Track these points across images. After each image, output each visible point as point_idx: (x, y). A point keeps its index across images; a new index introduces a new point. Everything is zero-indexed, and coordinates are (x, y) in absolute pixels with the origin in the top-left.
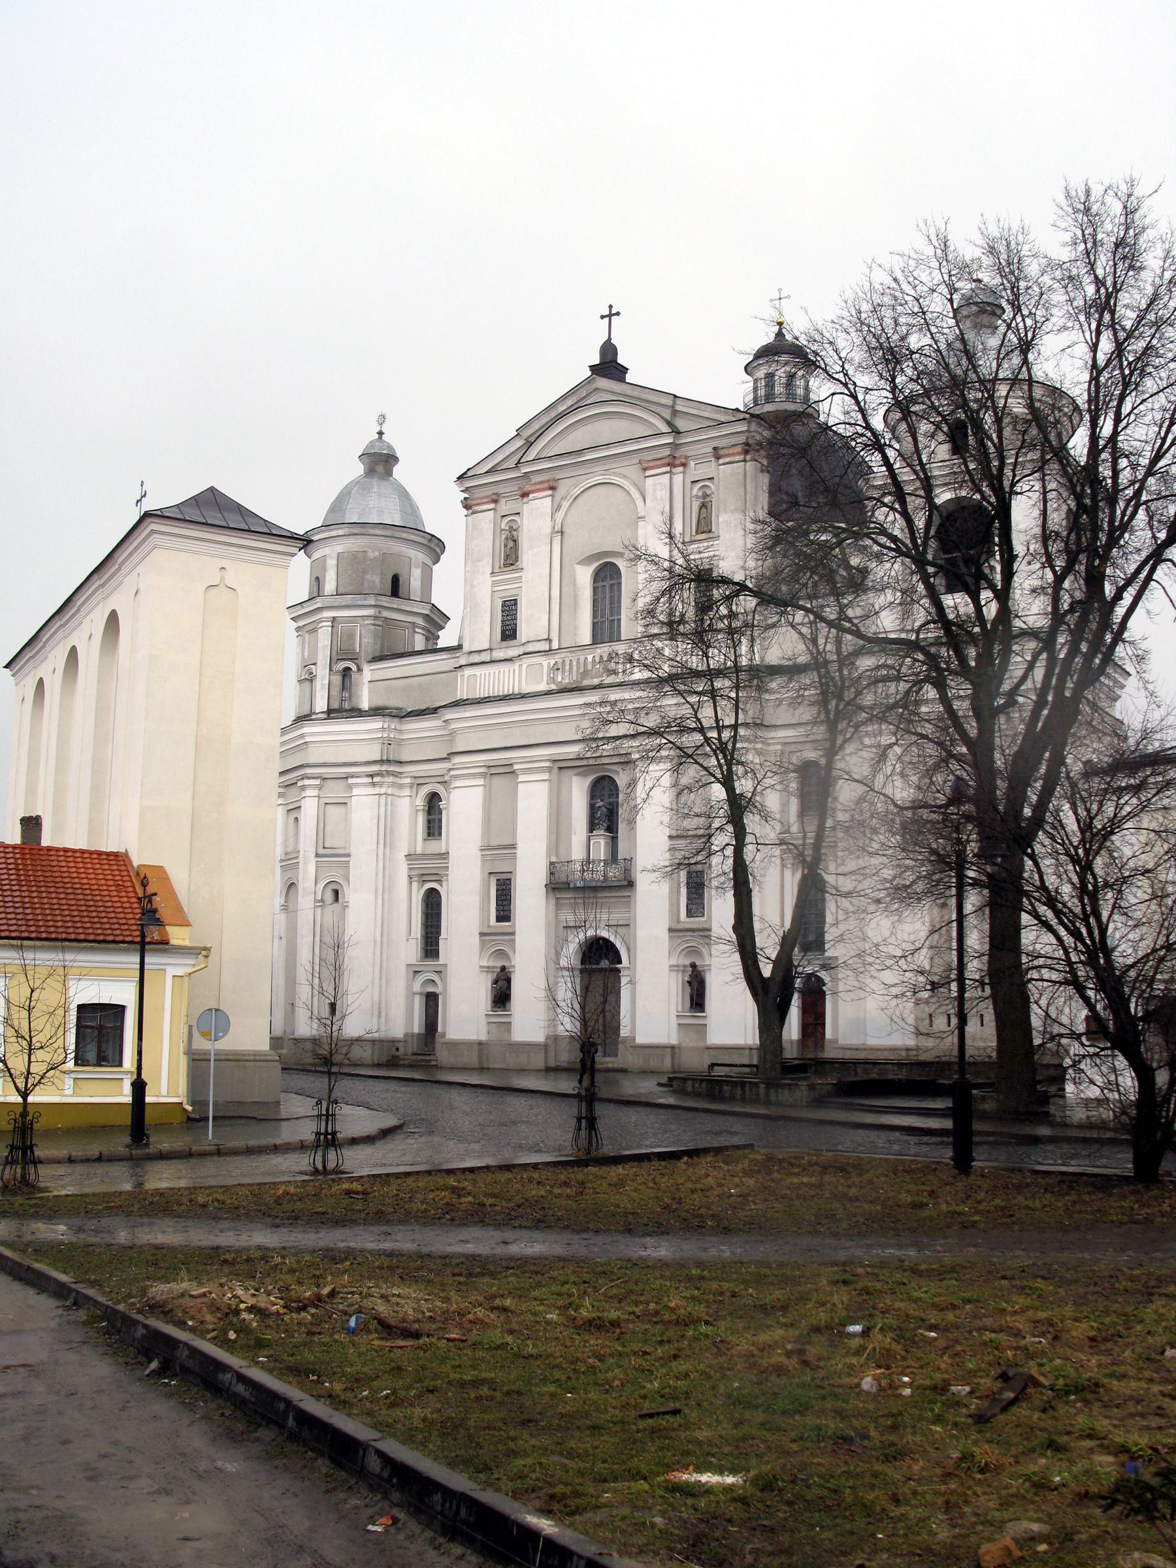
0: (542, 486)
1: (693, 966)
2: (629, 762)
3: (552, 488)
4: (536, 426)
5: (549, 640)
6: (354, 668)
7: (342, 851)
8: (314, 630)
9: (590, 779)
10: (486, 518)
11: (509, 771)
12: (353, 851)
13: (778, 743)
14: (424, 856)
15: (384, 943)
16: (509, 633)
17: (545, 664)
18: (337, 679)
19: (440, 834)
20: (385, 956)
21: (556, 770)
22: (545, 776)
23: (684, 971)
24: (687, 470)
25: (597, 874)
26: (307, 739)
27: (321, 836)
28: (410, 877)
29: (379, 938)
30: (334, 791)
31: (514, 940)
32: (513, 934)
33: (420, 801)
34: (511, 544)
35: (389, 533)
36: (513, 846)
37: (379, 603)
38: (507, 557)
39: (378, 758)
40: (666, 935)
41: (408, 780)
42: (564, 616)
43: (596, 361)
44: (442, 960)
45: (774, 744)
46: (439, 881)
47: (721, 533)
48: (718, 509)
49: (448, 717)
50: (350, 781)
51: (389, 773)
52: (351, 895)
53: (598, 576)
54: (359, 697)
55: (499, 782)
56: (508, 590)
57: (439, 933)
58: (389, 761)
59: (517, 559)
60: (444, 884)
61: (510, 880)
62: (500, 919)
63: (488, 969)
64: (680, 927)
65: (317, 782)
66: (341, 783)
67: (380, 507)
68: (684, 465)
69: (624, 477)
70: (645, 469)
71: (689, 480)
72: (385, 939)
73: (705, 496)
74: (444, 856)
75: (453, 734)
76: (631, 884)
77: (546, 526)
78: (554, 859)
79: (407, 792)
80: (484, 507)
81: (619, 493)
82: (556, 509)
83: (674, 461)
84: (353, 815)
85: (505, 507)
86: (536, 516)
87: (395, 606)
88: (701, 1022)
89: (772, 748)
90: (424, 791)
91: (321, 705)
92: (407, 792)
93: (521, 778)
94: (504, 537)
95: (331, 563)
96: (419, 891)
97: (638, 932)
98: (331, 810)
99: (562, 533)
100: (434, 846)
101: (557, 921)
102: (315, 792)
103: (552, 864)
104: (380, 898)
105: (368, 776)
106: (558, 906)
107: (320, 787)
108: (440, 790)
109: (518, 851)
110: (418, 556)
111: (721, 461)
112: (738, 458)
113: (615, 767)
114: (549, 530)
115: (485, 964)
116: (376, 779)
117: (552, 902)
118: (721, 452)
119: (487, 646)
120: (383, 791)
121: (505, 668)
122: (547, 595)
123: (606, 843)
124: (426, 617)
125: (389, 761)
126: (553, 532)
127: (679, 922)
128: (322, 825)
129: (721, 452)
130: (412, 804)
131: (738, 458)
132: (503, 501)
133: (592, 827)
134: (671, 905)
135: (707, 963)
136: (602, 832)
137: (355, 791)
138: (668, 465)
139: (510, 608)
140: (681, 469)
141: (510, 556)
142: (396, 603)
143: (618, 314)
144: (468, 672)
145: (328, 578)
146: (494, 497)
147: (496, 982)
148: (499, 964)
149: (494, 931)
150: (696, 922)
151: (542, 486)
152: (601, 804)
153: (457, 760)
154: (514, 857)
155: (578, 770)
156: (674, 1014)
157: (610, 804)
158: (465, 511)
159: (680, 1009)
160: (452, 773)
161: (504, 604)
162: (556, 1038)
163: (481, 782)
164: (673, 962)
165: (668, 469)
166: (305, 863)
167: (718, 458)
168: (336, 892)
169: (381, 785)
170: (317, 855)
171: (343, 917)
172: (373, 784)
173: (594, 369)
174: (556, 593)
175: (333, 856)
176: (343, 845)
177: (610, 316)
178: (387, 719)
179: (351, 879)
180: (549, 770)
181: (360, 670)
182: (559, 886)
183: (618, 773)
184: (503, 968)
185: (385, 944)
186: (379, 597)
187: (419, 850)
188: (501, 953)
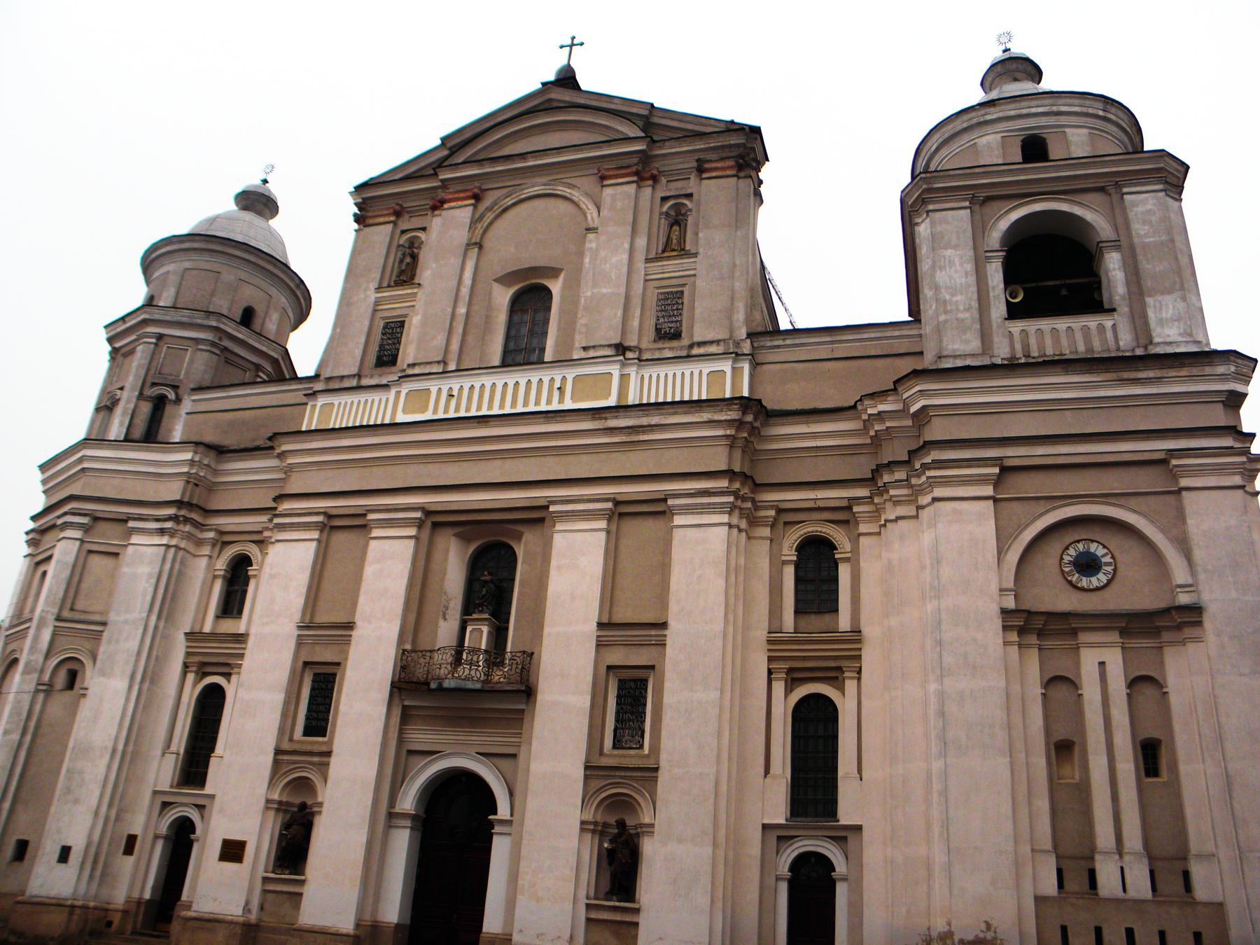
0: (462, 195)
1: (621, 824)
3: (477, 198)
4: (467, 135)
5: (444, 362)
6: (172, 396)
7: (97, 618)
8: (132, 352)
10: (381, 234)
11: (359, 524)
12: (112, 617)
13: (772, 507)
14: (213, 636)
15: (129, 754)
16: (387, 357)
17: (434, 390)
18: (146, 408)
19: (240, 612)
20: (124, 775)
21: (428, 524)
22: (412, 531)
23: (602, 834)
24: (658, 187)
25: (472, 674)
26: (86, 465)
27: (71, 594)
28: (186, 666)
29: (120, 747)
30: (107, 536)
31: (328, 764)
33: (221, 564)
34: (408, 260)
35: (252, 258)
36: (350, 626)
37: (222, 326)
38: (401, 272)
39: (178, 497)
40: (581, 773)
41: (211, 535)
42: (470, 339)
43: (552, 78)
44: (208, 790)
45: (766, 508)
46: (227, 676)
47: (701, 250)
48: (697, 225)
49: (285, 448)
50: (131, 524)
51: (187, 520)
52: (92, 680)
53: (517, 304)
54: (170, 431)
55: (340, 538)
56: (393, 309)
57: (212, 749)
58: (190, 506)
59: (413, 276)
60: (234, 678)
61: (335, 675)
62: (308, 732)
63: (281, 807)
65: (85, 520)
66: (118, 528)
67: (248, 228)
68: (655, 179)
69: (572, 186)
70: (603, 178)
71: (660, 193)
72: (130, 748)
73: (678, 213)
74: (241, 638)
75: (289, 470)
76: (528, 692)
77: (460, 235)
78: (408, 647)
79: (206, 550)
80: (381, 220)
81: (563, 206)
82: (474, 222)
83: (643, 170)
84: (126, 569)
85: (404, 225)
86: (447, 229)
87: (240, 336)
88: (628, 918)
89: (763, 513)
90: (230, 552)
91: (116, 429)
92: (206, 550)
94: (400, 254)
95: (173, 279)
96: (195, 685)
97: (534, 766)
98: (95, 561)
99: (480, 247)
100: (228, 626)
101: (401, 740)
102: (78, 534)
104: (136, 688)
105: (158, 520)
106: (407, 717)
107: (87, 529)
108: (253, 551)
109: (355, 633)
110: (283, 300)
111: (704, 176)
112: (729, 172)
113: (519, 528)
114: (465, 241)
115: (276, 797)
116: (168, 525)
117: (397, 712)
118: (707, 166)
119: (354, 370)
120: (174, 542)
121: (376, 396)
122: (450, 310)
123: (490, 633)
124: (275, 362)
125: (190, 506)
126: (469, 245)
127: (601, 753)
128: (76, 579)
129: (707, 166)
130: (210, 567)
131: (729, 172)
132: (406, 216)
133: (469, 608)
134: (591, 726)
135: (647, 820)
137: (135, 539)
138: (637, 173)
139: (393, 331)
140: (650, 182)
141: (405, 270)
142: (242, 333)
143: (582, 44)
144: (321, 401)
145: (165, 294)
146: (398, 208)
147: (287, 826)
148: (297, 801)
149: (296, 747)
150: (629, 758)
151: (462, 195)
152: (488, 578)
153: (286, 506)
154: (347, 640)
155: (459, 530)
156: (583, 902)
157: (501, 580)
158: (356, 226)
159: (592, 894)
160: (276, 521)
161: (386, 326)
163: (316, 535)
164: (589, 816)
165: (635, 178)
166: (39, 628)
167: (700, 170)
168: (73, 678)
169: (172, 533)
170: (59, 619)
171: (73, 711)
172: (162, 532)
173: (544, 84)
174: (462, 310)
175: (79, 625)
176: (96, 608)
178: (201, 449)
179: (100, 657)
180: (420, 524)
181: (178, 400)
182: (412, 688)
183: (518, 537)
184: (303, 806)
185: (128, 758)
186: (224, 320)
187: (207, 628)
188: (304, 785)
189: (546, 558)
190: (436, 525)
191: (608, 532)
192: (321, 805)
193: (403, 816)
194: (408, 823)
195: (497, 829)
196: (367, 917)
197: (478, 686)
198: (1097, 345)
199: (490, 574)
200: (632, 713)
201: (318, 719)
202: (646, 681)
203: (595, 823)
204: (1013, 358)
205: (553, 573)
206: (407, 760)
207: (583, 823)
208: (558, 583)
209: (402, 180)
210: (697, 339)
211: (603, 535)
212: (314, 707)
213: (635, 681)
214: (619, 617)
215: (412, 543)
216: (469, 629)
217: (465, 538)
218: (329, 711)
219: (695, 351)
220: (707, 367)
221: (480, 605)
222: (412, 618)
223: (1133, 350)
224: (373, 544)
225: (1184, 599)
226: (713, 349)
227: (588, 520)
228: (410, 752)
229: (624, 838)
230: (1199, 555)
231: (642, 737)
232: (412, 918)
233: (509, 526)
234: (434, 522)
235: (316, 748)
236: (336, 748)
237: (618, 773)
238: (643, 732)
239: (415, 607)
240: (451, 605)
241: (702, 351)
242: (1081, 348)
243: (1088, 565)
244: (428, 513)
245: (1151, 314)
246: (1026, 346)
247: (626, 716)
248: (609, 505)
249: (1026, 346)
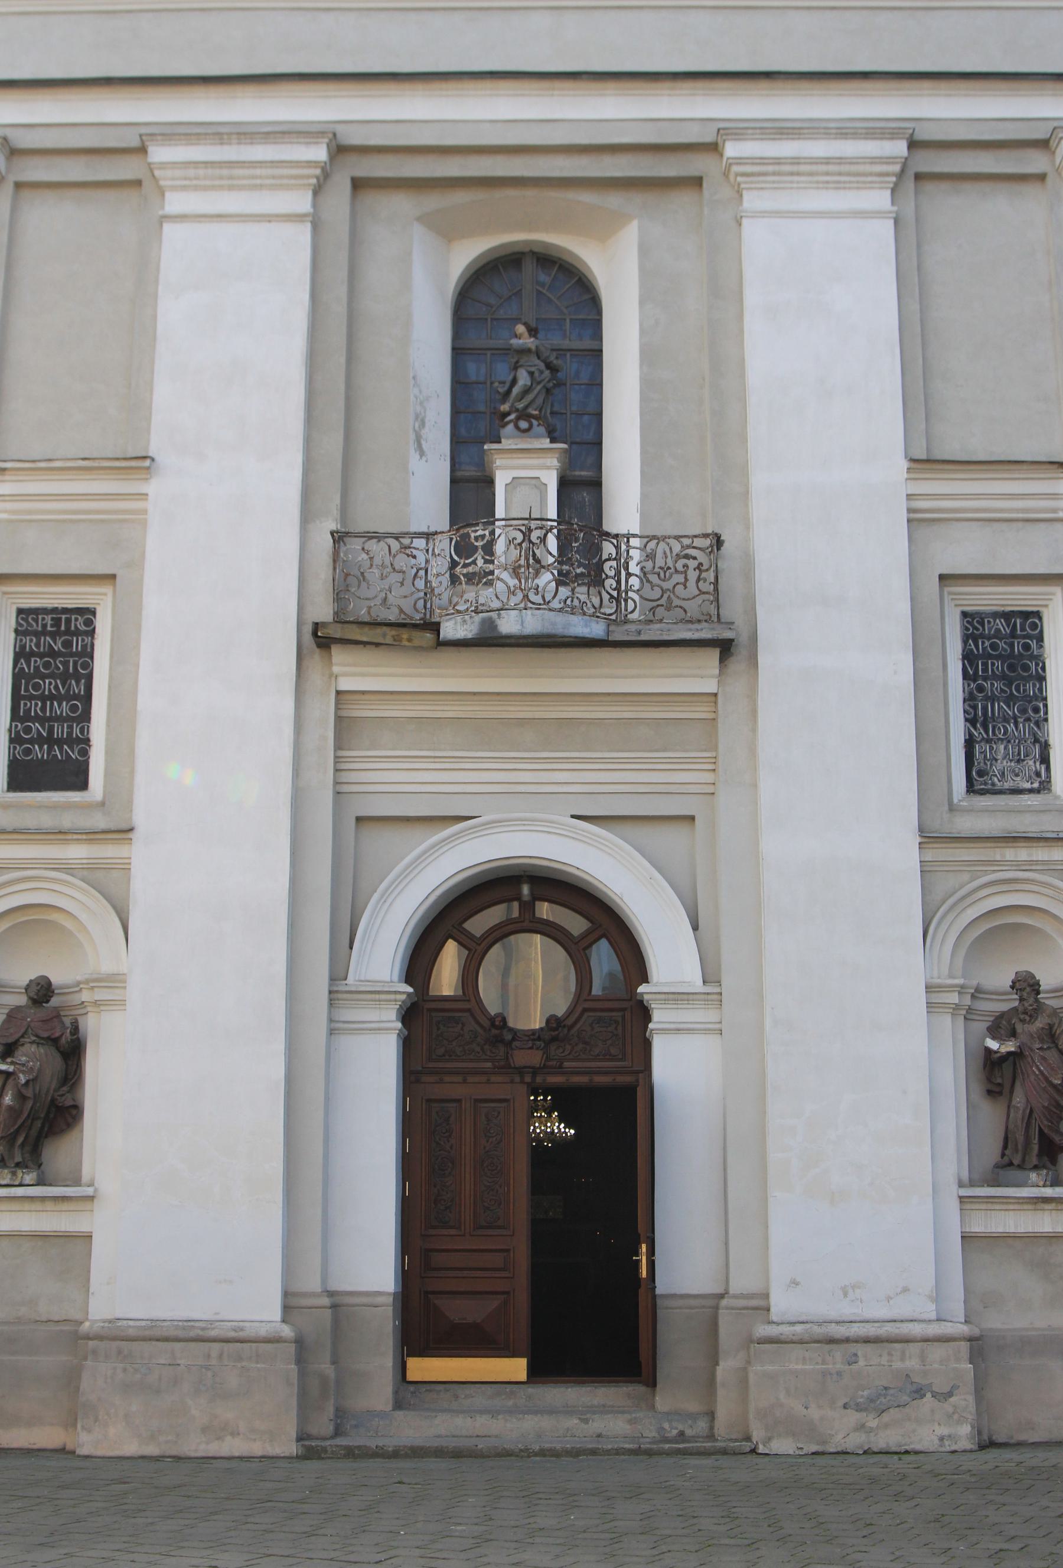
2: (697, 182)
9: (465, 255)
32: (125, 832)
61: (88, 614)
64: (965, 824)
93: (175, 203)
103: (339, 538)
106: (345, 729)
113: (614, 200)
117: (322, 710)
136: (546, 443)
155: (433, 201)
156: (951, 1192)
157: (560, 352)
162: (340, 1307)
183: (604, 228)
189: (724, 290)
190: (358, 185)
191: (896, 222)
192: (116, 980)
193: (374, 994)
194: (390, 1017)
195: (660, 1017)
196: (311, 1283)
197: (596, 629)
199: (533, 332)
200: (1010, 700)
201: (50, 740)
202: (1038, 615)
203: (961, 989)
205: (754, 325)
206: (357, 839)
207: (929, 988)
208: (770, 353)
211: (886, 229)
212: (35, 707)
213: (1008, 616)
214: (938, 455)
215: (303, 234)
216: (501, 480)
217: (447, 230)
218: (86, 716)
221: (524, 415)
222: (332, 444)
224: (167, 227)
227: (839, 186)
228: (359, 819)
229: (1040, 1023)
231: (1045, 760)
232: (406, 1276)
233: (587, 197)
234: (360, 175)
235: (67, 821)
236: (140, 818)
237: (1010, 854)
238: (1045, 747)
239: (336, 416)
240: (431, 417)
244: (340, 150)
247: (999, 707)
248: (900, 148)
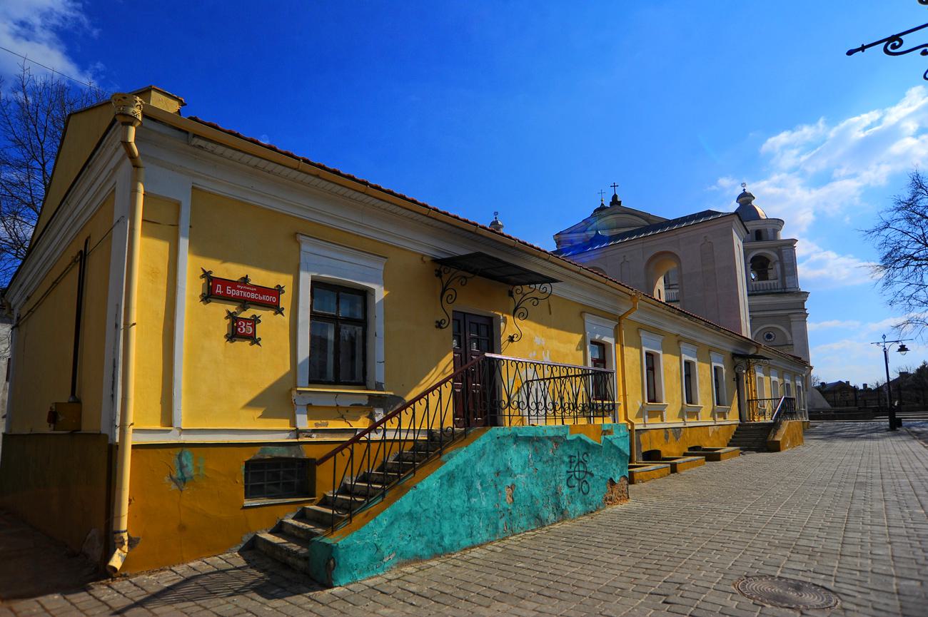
177: (614, 186)
198: (773, 287)
204: (753, 291)
209: (569, 233)
210: (671, 283)
219: (671, 287)
220: (675, 291)
223: (781, 289)
225: (790, 343)
226: (675, 286)
230: (793, 335)
241: (673, 287)
242: (769, 288)
243: (769, 336)
245: (787, 280)
246: (756, 288)
249: (756, 288)
